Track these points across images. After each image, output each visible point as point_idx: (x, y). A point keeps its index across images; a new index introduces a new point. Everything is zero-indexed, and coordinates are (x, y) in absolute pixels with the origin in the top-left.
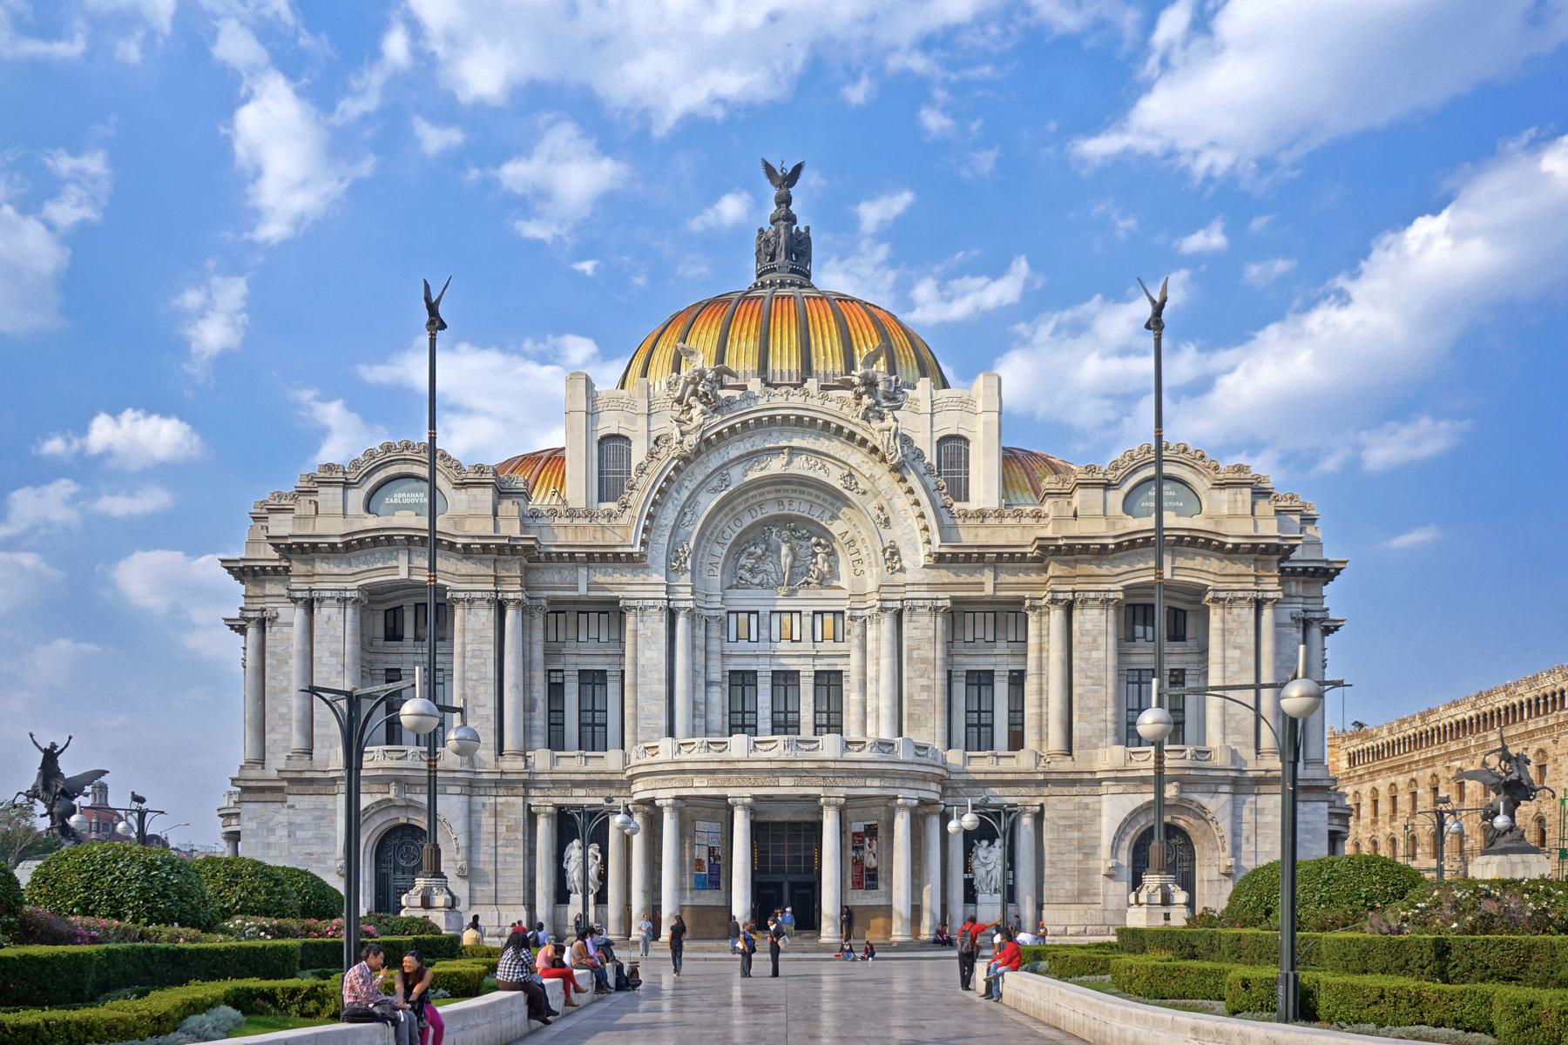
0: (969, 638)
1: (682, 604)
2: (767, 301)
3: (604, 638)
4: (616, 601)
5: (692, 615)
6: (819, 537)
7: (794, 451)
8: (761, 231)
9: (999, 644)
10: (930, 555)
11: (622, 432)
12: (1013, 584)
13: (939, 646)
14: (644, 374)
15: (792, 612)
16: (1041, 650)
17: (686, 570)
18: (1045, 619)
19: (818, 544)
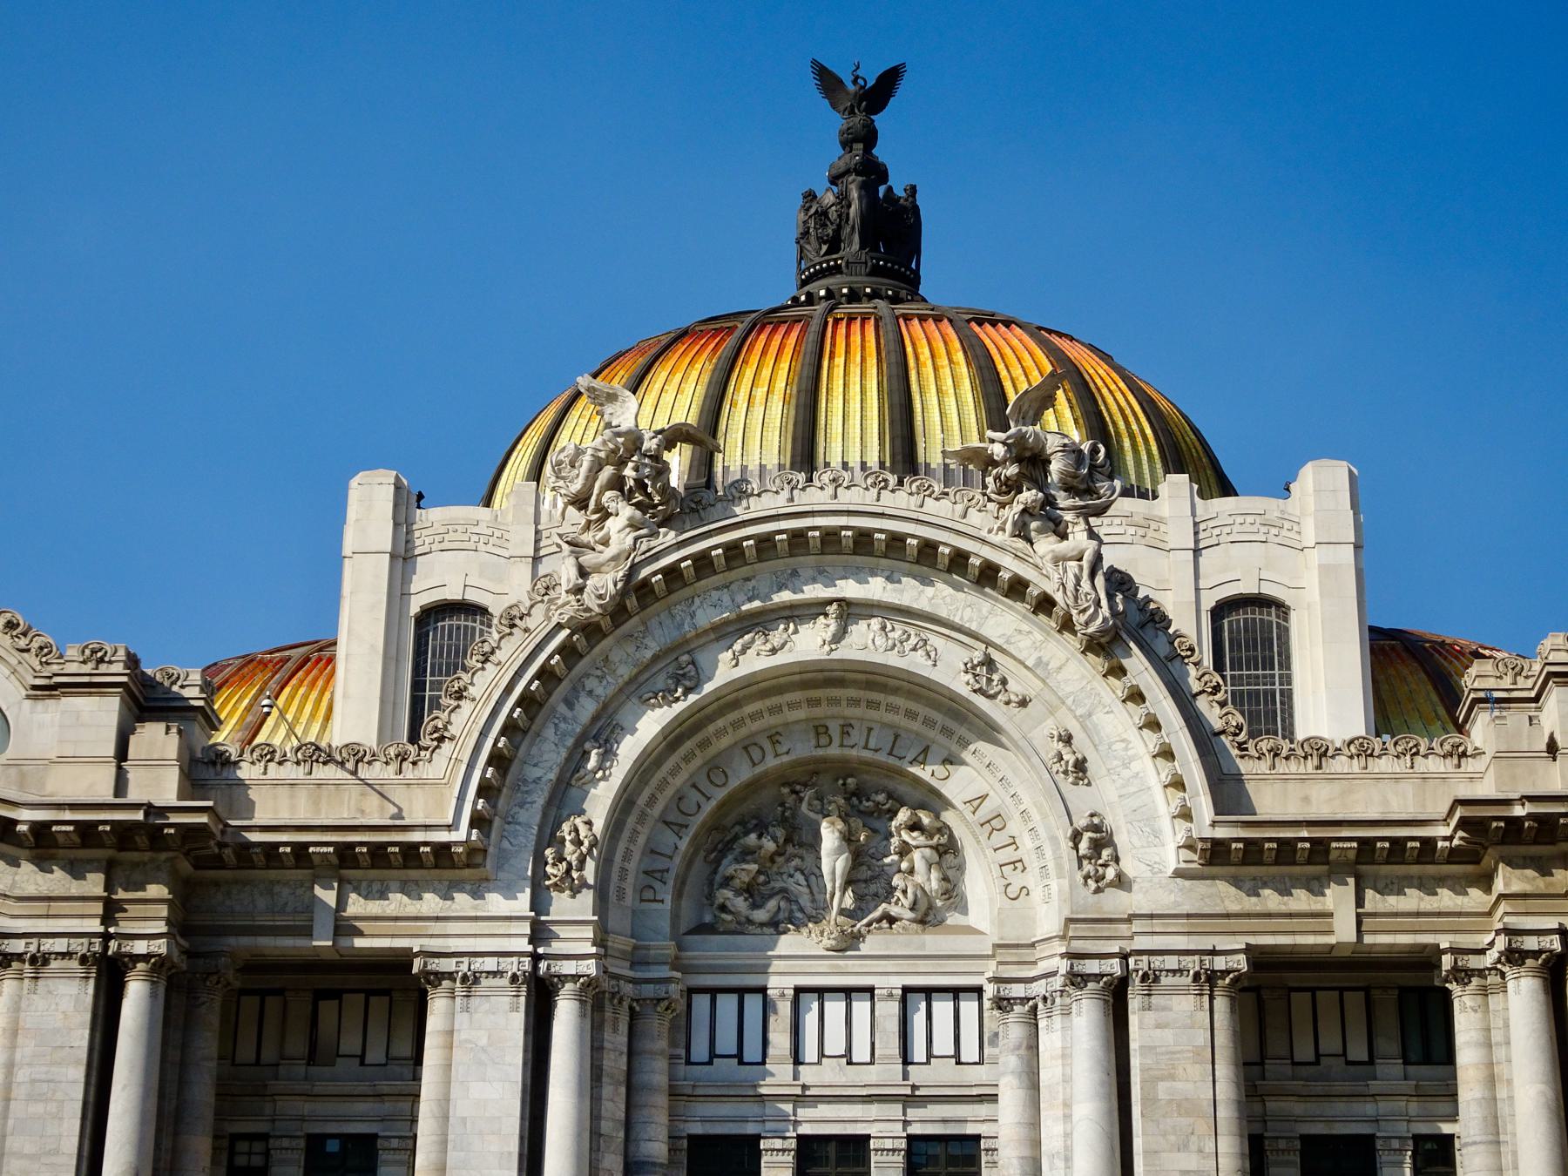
0: (1304, 1052)
1: (568, 968)
2: (815, 326)
3: (375, 1055)
4: (406, 957)
5: (595, 999)
6: (915, 807)
7: (850, 611)
8: (810, 196)
9: (1381, 1068)
10: (1189, 846)
11: (473, 596)
12: (1408, 917)
13: (1224, 1070)
14: (536, 474)
15: (848, 992)
16: (1491, 1081)
17: (584, 884)
18: (1495, 1001)
19: (915, 826)
